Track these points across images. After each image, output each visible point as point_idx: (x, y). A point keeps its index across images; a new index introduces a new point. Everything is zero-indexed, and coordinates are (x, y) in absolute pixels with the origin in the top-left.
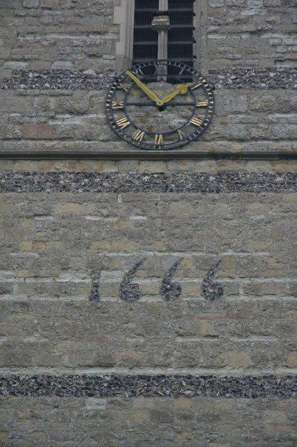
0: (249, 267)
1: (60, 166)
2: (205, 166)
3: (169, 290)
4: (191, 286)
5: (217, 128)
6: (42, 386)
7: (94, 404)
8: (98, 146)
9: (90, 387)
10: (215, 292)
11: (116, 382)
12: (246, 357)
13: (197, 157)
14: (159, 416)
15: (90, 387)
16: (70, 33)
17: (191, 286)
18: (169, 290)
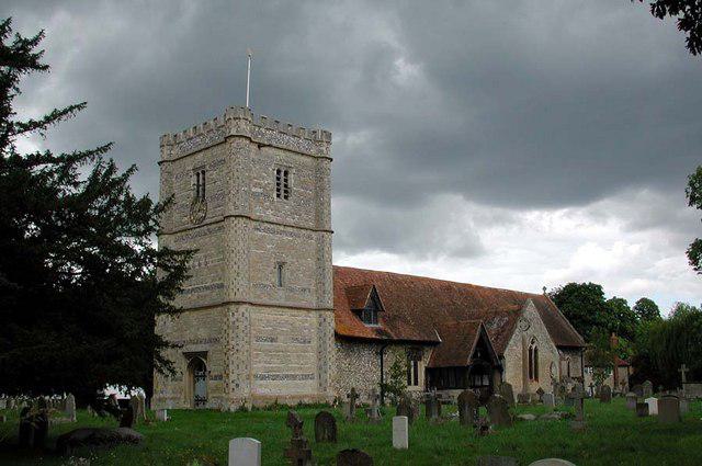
4: (202, 262)
11: (193, 289)
17: (202, 262)
18: (200, 265)
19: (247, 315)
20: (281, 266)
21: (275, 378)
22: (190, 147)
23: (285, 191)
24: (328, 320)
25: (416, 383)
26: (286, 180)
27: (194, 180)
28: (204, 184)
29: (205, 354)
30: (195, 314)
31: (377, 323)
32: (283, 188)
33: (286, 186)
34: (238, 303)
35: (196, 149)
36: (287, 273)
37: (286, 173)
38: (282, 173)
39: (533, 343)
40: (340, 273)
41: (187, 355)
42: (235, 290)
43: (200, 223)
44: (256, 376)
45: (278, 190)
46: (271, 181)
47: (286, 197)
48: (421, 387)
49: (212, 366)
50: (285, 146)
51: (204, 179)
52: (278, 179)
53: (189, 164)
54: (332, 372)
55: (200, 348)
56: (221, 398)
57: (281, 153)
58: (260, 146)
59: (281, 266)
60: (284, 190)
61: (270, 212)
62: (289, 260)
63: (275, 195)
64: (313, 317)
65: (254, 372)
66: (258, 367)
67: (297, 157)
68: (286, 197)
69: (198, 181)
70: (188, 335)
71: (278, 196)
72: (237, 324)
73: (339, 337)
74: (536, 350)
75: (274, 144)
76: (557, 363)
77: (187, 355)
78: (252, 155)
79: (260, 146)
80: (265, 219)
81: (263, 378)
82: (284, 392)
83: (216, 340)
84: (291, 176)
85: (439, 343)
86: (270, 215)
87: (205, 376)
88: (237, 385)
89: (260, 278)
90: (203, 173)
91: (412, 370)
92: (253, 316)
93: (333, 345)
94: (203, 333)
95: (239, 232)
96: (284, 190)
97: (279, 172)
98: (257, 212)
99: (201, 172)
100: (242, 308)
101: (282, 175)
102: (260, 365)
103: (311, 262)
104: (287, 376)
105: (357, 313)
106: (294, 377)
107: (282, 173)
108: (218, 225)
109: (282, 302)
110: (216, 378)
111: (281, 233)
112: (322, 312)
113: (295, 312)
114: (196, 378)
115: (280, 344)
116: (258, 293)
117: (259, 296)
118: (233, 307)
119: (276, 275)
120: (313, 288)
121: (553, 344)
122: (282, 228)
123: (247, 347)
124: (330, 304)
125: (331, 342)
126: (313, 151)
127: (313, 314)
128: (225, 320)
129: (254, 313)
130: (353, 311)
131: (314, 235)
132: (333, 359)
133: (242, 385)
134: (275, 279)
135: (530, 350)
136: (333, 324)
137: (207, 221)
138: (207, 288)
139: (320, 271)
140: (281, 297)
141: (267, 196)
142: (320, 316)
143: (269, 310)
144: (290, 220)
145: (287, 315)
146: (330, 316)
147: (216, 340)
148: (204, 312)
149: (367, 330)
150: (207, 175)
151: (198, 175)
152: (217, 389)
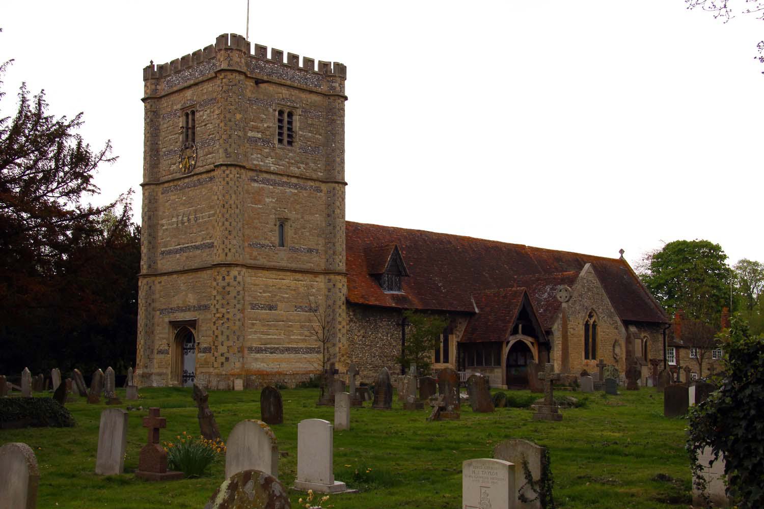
0: (202, 211)
1: (171, 184)
2: (195, 178)
3: (189, 220)
4: (192, 217)
5: (198, 164)
6: (170, 252)
7: (178, 256)
8: (178, 176)
9: (177, 252)
10: (196, 219)
11: (181, 249)
12: (200, 239)
13: (193, 175)
14: (187, 258)
15: (177, 252)
16: (173, 135)
17: (192, 217)
18: (189, 220)
19: (239, 279)
20: (282, 223)
21: (273, 351)
22: (177, 81)
23: (290, 136)
24: (339, 285)
25: (446, 360)
26: (290, 123)
27: (181, 122)
28: (194, 127)
29: (193, 323)
30: (183, 278)
31: (399, 289)
32: (286, 132)
33: (290, 129)
34: (229, 265)
35: (186, 85)
36: (289, 232)
37: (290, 115)
38: (286, 115)
39: (590, 316)
40: (355, 229)
41: (174, 324)
42: (227, 251)
43: (190, 172)
44: (250, 349)
45: (280, 134)
46: (273, 124)
47: (290, 143)
48: (452, 365)
49: (203, 337)
50: (289, 82)
51: (193, 120)
52: (280, 121)
53: (177, 103)
54: (342, 343)
55: (187, 316)
56: (210, 374)
57: (284, 91)
58: (258, 82)
59: (282, 223)
60: (287, 135)
61: (269, 160)
62: (292, 215)
63: (276, 142)
64: (320, 283)
65: (248, 344)
66: (253, 338)
67: (303, 96)
68: (290, 143)
69: (187, 122)
70: (177, 301)
71: (280, 141)
72: (228, 289)
73: (349, 304)
74: (594, 326)
75: (274, 78)
76: (623, 342)
77: (174, 324)
78: (249, 94)
79: (258, 82)
80: (264, 169)
81: (259, 351)
82: (285, 367)
83: (206, 308)
84: (296, 118)
85: (475, 313)
86: (270, 163)
87: (193, 348)
88: (227, 359)
89: (256, 238)
90: (193, 113)
91: (442, 345)
92: (248, 280)
93: (344, 315)
94: (192, 299)
95: (231, 183)
96: (287, 135)
97: (281, 113)
98: (256, 160)
99: (190, 113)
100: (234, 272)
101: (285, 119)
102: (255, 336)
103: (318, 218)
104: (288, 350)
105: (376, 277)
106: (296, 351)
107: (286, 115)
108: (209, 175)
109: (284, 264)
110: (207, 350)
111: (283, 184)
112: (332, 276)
113: (298, 276)
114: (184, 351)
115: (280, 312)
116: (255, 253)
117: (255, 259)
118: (223, 270)
119: (277, 233)
120: (320, 248)
121: (617, 319)
122: (285, 179)
123: (239, 316)
124: (342, 267)
125: (342, 315)
126: (324, 88)
127: (321, 278)
128: (215, 283)
129: (248, 277)
130: (371, 275)
131: (324, 187)
132: (344, 331)
133: (232, 359)
134: (276, 239)
135: (587, 325)
136: (345, 290)
137: (197, 170)
138: (197, 247)
139: (331, 228)
140: (282, 258)
141: (266, 141)
142: (330, 280)
143: (265, 272)
144: (294, 170)
145: (288, 280)
146: (342, 284)
147: (206, 308)
148: (194, 275)
149: (388, 295)
150: (197, 115)
151: (187, 115)
152: (206, 363)
